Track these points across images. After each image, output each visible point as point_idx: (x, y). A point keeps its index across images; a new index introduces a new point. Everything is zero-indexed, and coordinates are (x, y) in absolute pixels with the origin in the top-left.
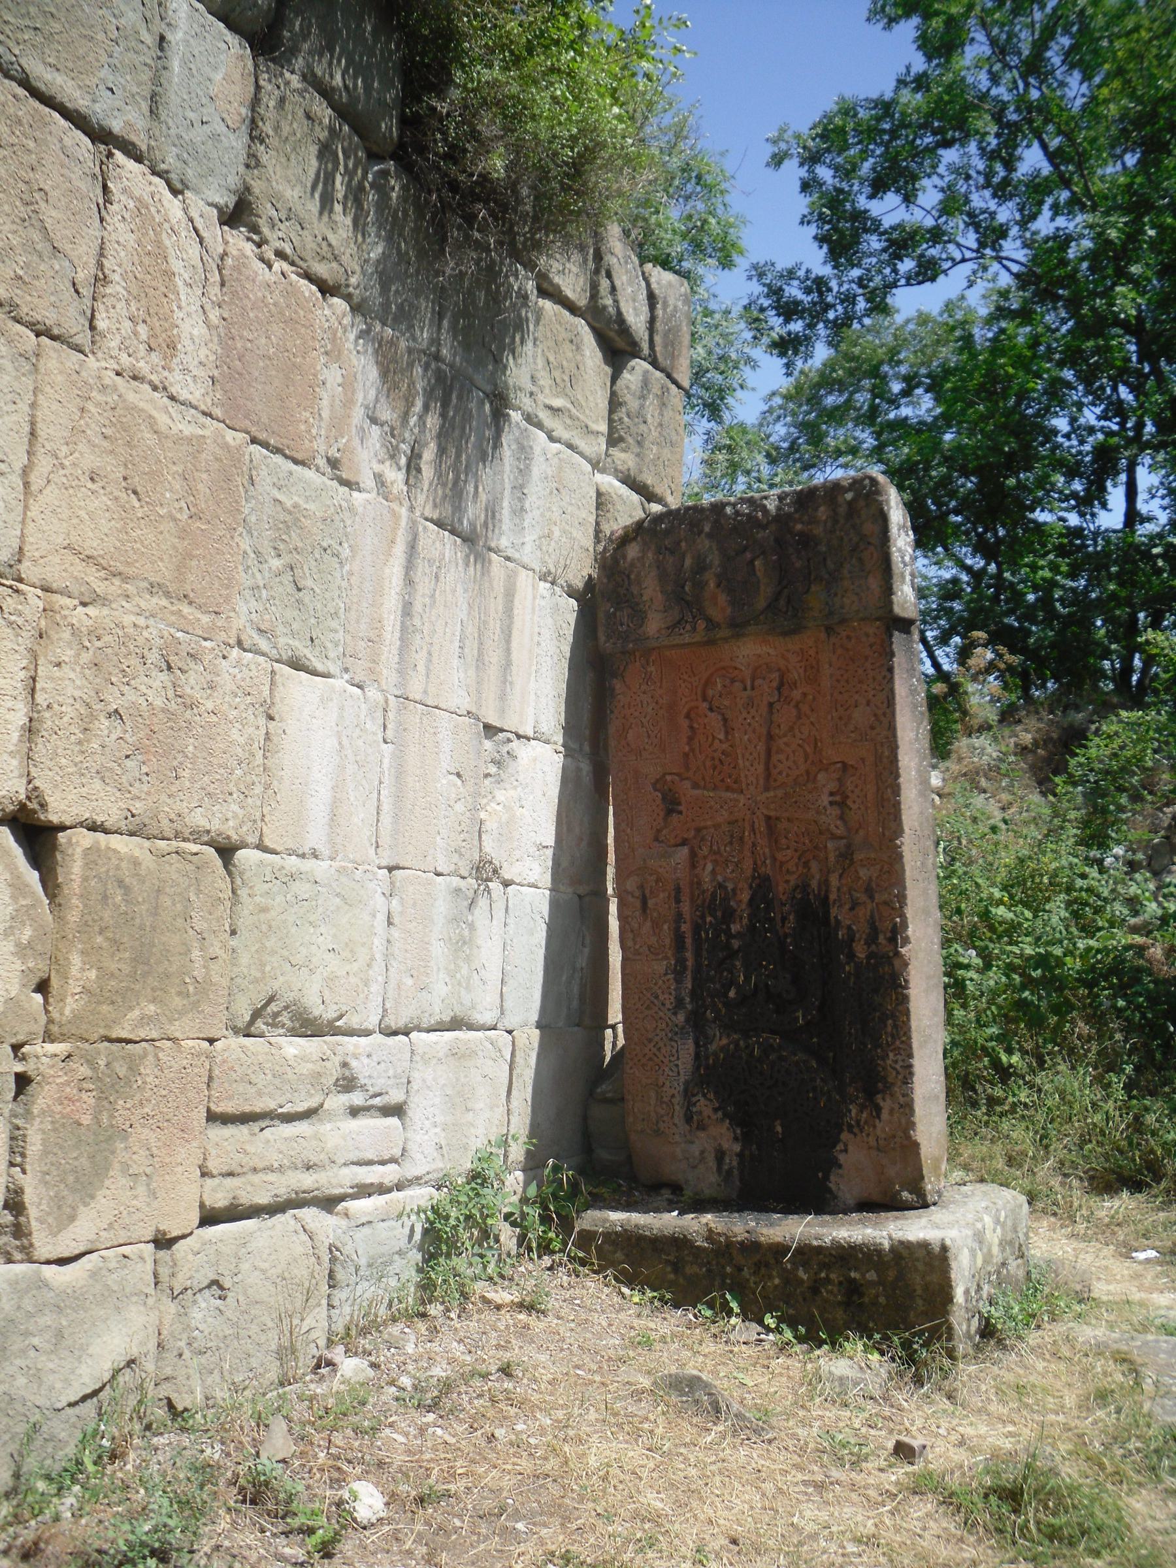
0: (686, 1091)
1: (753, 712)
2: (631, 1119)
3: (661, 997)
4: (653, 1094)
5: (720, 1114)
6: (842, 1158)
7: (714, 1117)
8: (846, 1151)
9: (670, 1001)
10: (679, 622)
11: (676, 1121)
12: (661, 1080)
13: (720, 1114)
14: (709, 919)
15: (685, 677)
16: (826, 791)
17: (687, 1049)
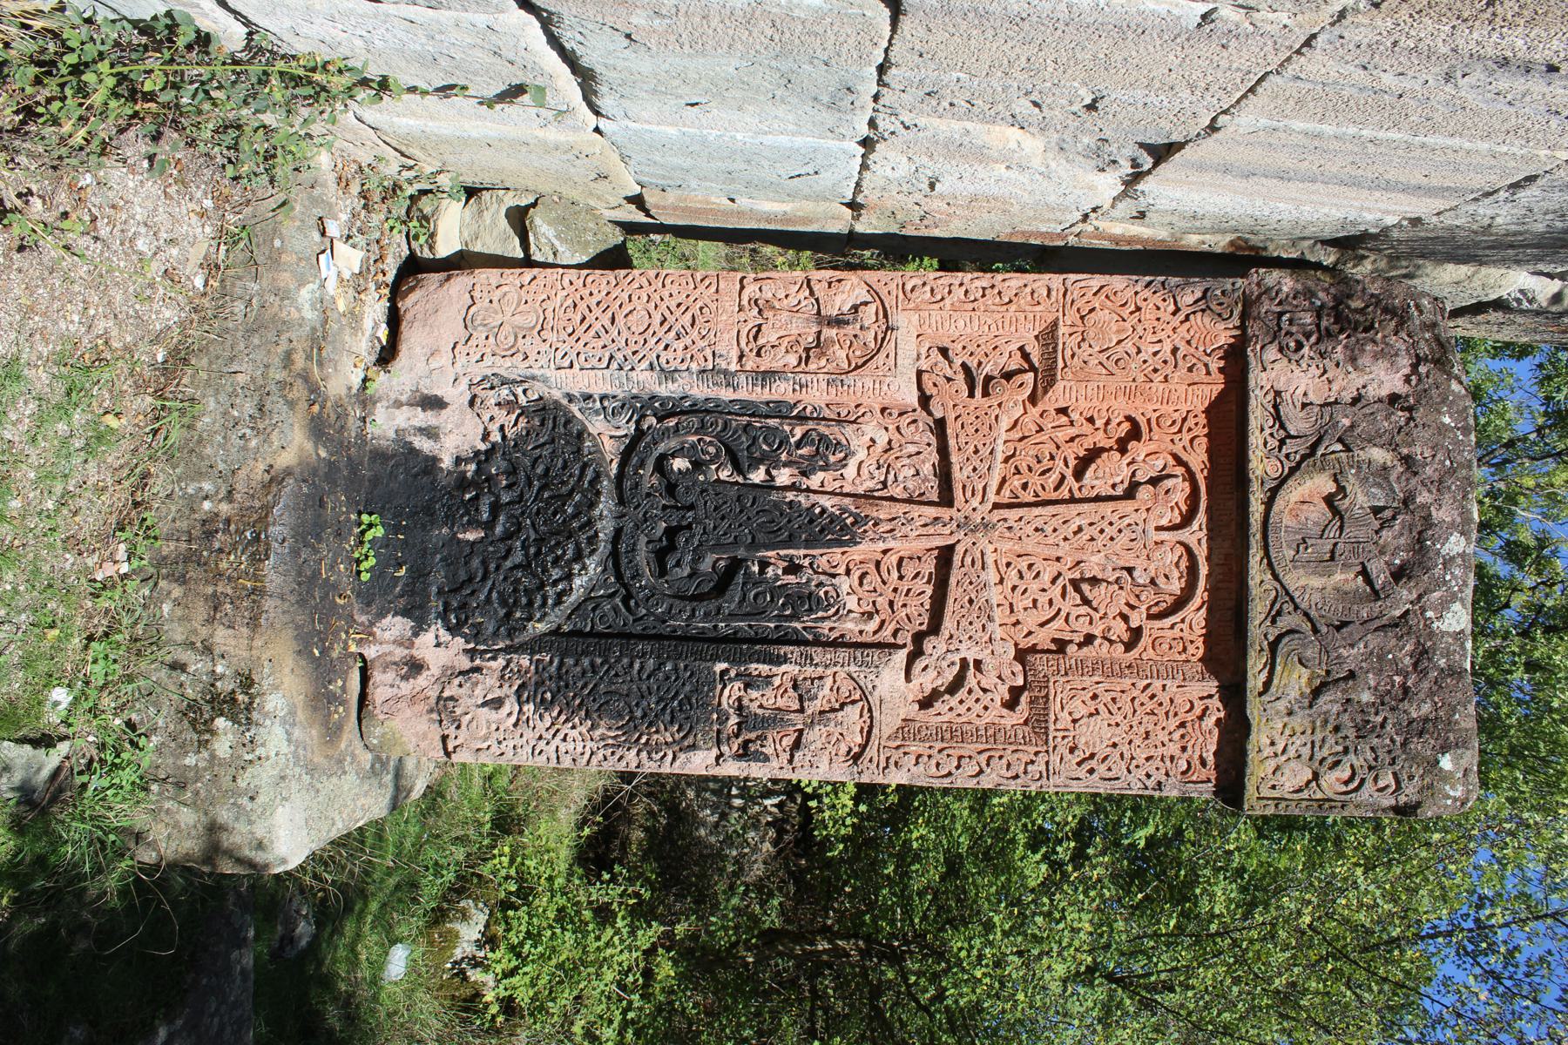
0: (534, 378)
1: (1123, 540)
2: (495, 280)
3: (680, 345)
4: (531, 319)
5: (496, 437)
6: (428, 638)
7: (494, 428)
8: (438, 645)
9: (671, 359)
10: (1282, 426)
11: (488, 360)
12: (551, 337)
13: (496, 437)
14: (799, 432)
15: (1191, 422)
16: (984, 655)
17: (599, 383)
